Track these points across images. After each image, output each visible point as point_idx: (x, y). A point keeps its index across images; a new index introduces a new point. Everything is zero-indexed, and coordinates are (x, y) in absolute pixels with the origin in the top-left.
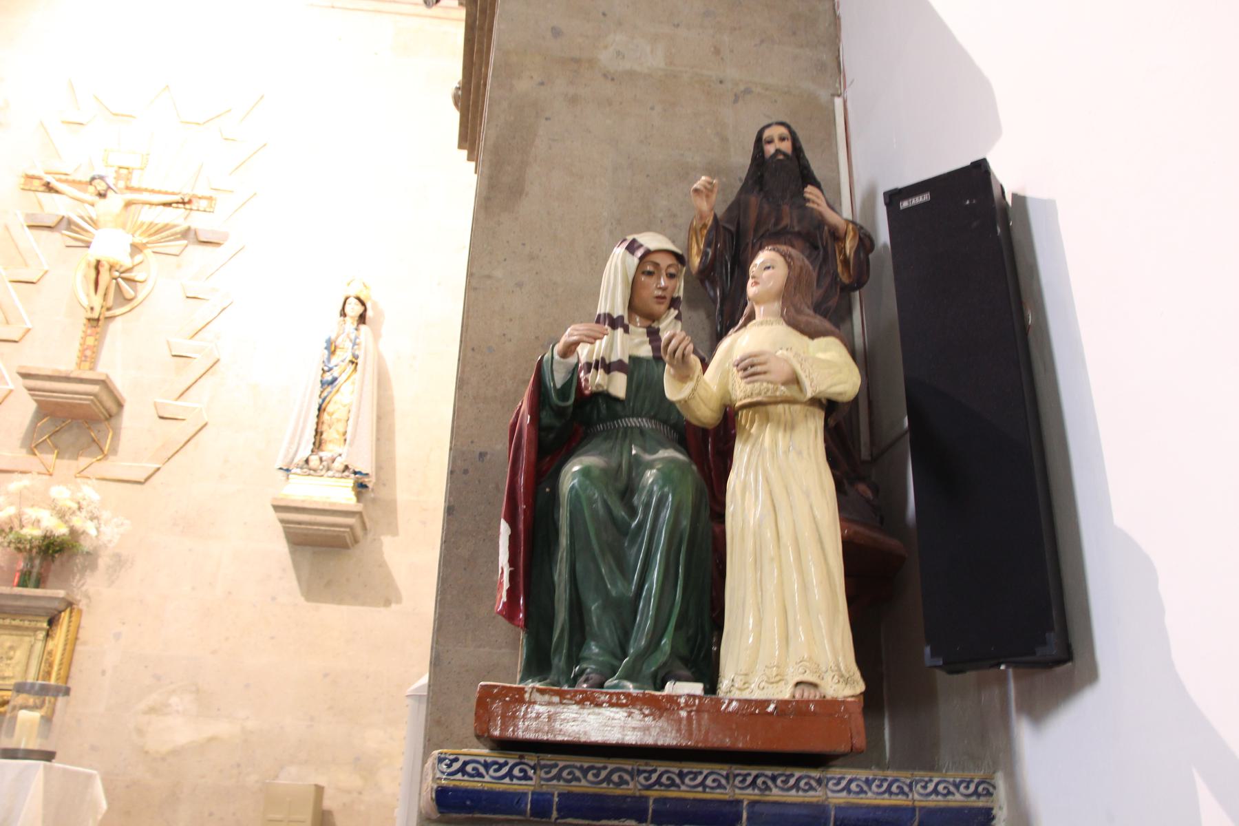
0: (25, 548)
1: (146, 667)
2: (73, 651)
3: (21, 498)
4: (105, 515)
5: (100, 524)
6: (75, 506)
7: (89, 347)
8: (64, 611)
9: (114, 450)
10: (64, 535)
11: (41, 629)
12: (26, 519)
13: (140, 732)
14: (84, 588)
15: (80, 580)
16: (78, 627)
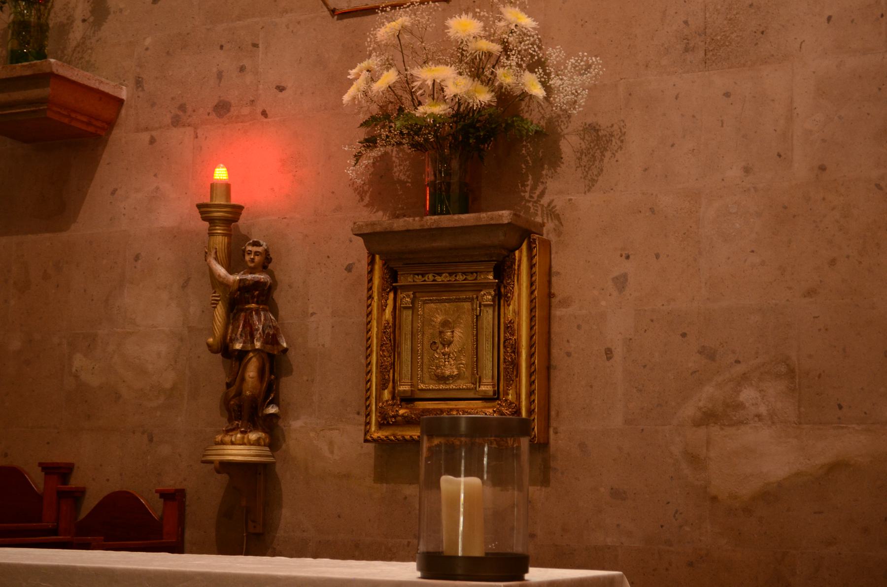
0: (426, 140)
1: (684, 335)
2: (548, 318)
4: (554, 54)
5: (549, 75)
6: (496, 48)
8: (519, 247)
10: (490, 106)
11: (487, 285)
12: (420, 88)
13: (695, 460)
14: (545, 201)
15: (534, 188)
16: (549, 273)
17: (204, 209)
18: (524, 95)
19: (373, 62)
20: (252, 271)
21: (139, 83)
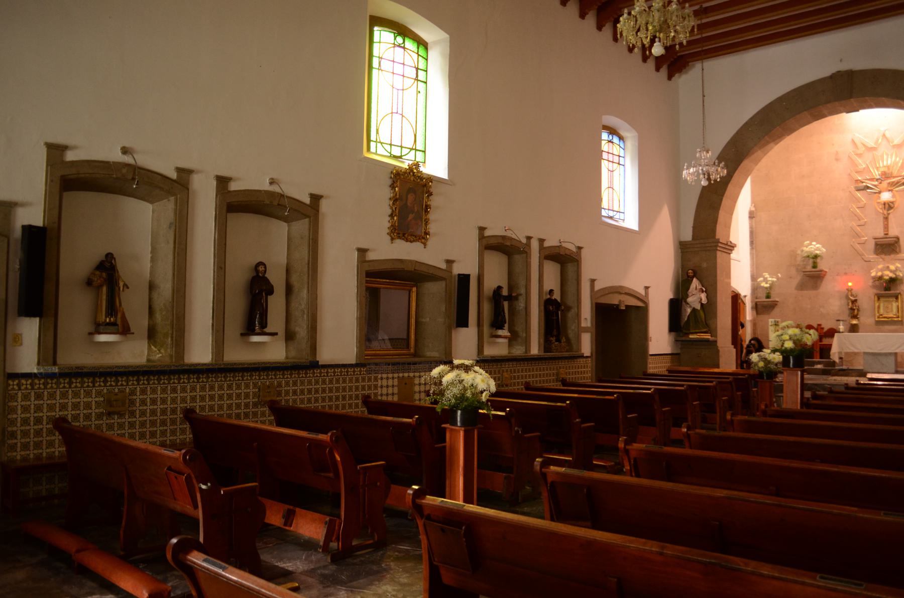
3: (881, 270)
7: (885, 225)
9: (900, 251)
17: (848, 290)
18: (899, 275)
19: (875, 270)
20: (854, 297)
21: (830, 269)
